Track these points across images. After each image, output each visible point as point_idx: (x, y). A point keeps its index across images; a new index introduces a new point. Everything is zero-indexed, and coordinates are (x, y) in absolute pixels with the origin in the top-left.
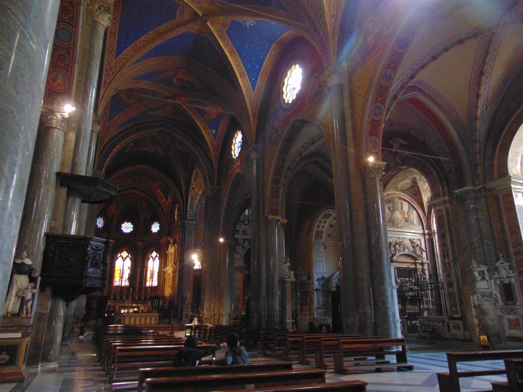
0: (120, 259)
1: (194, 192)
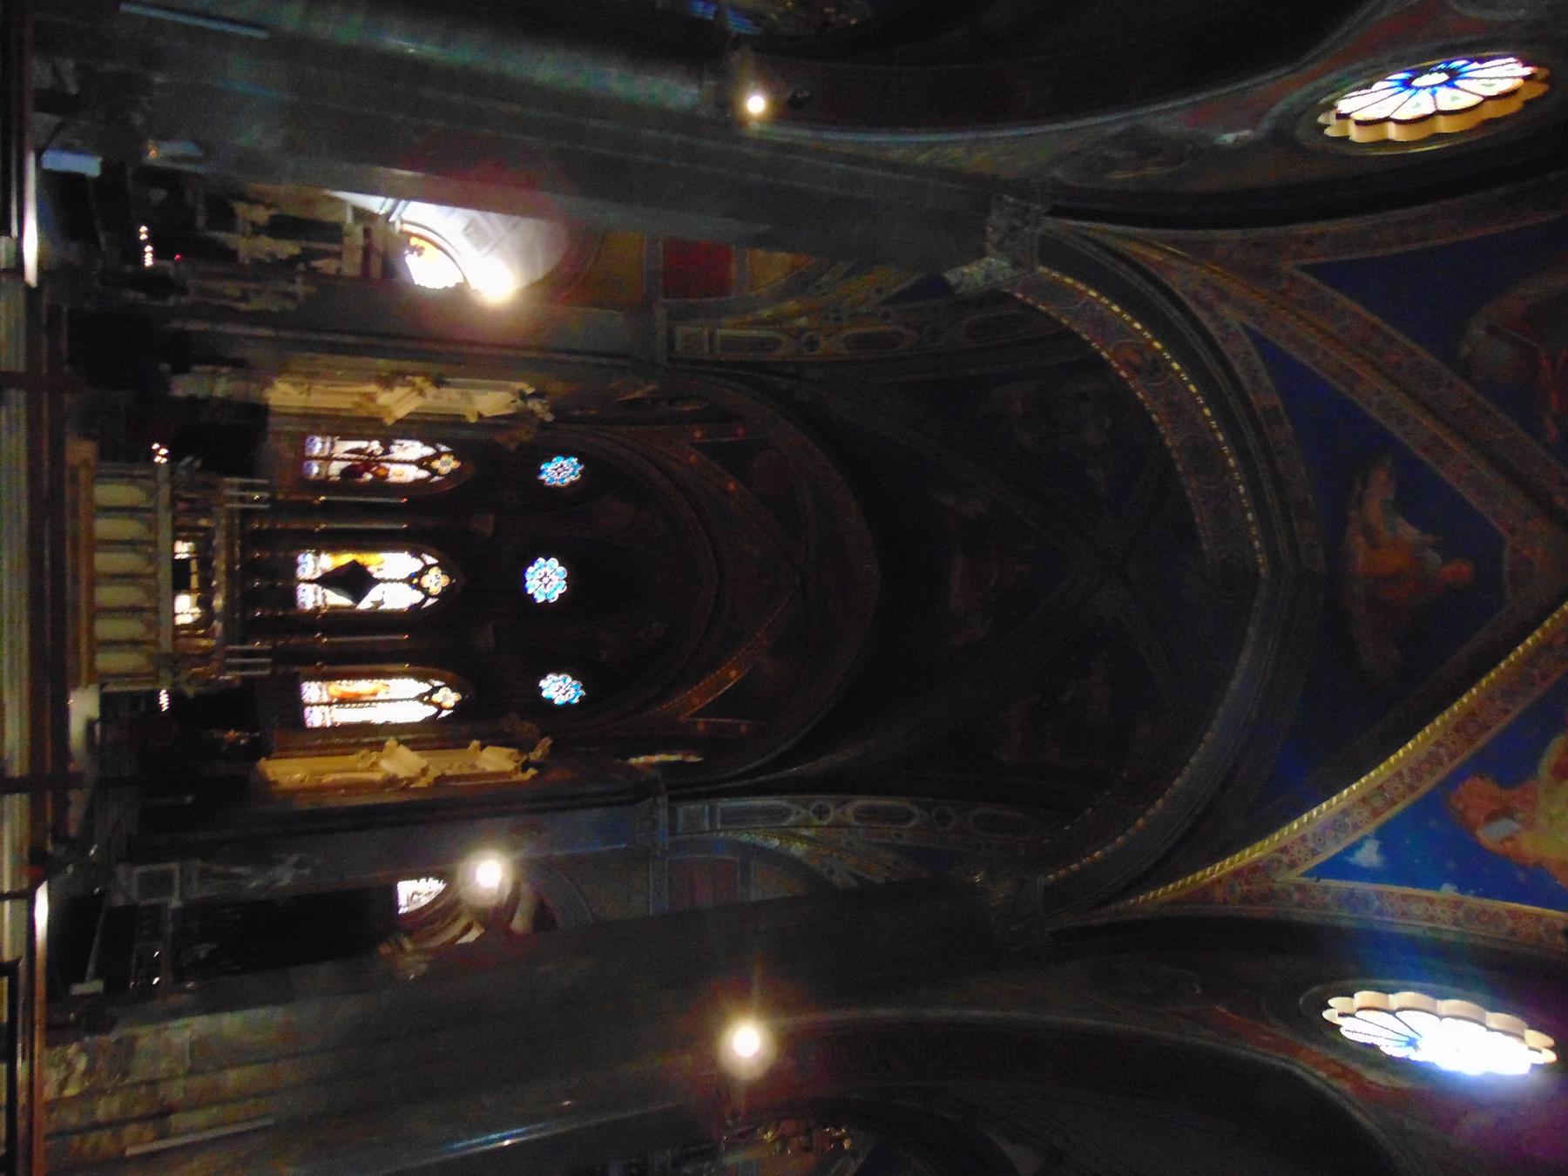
0: (416, 565)
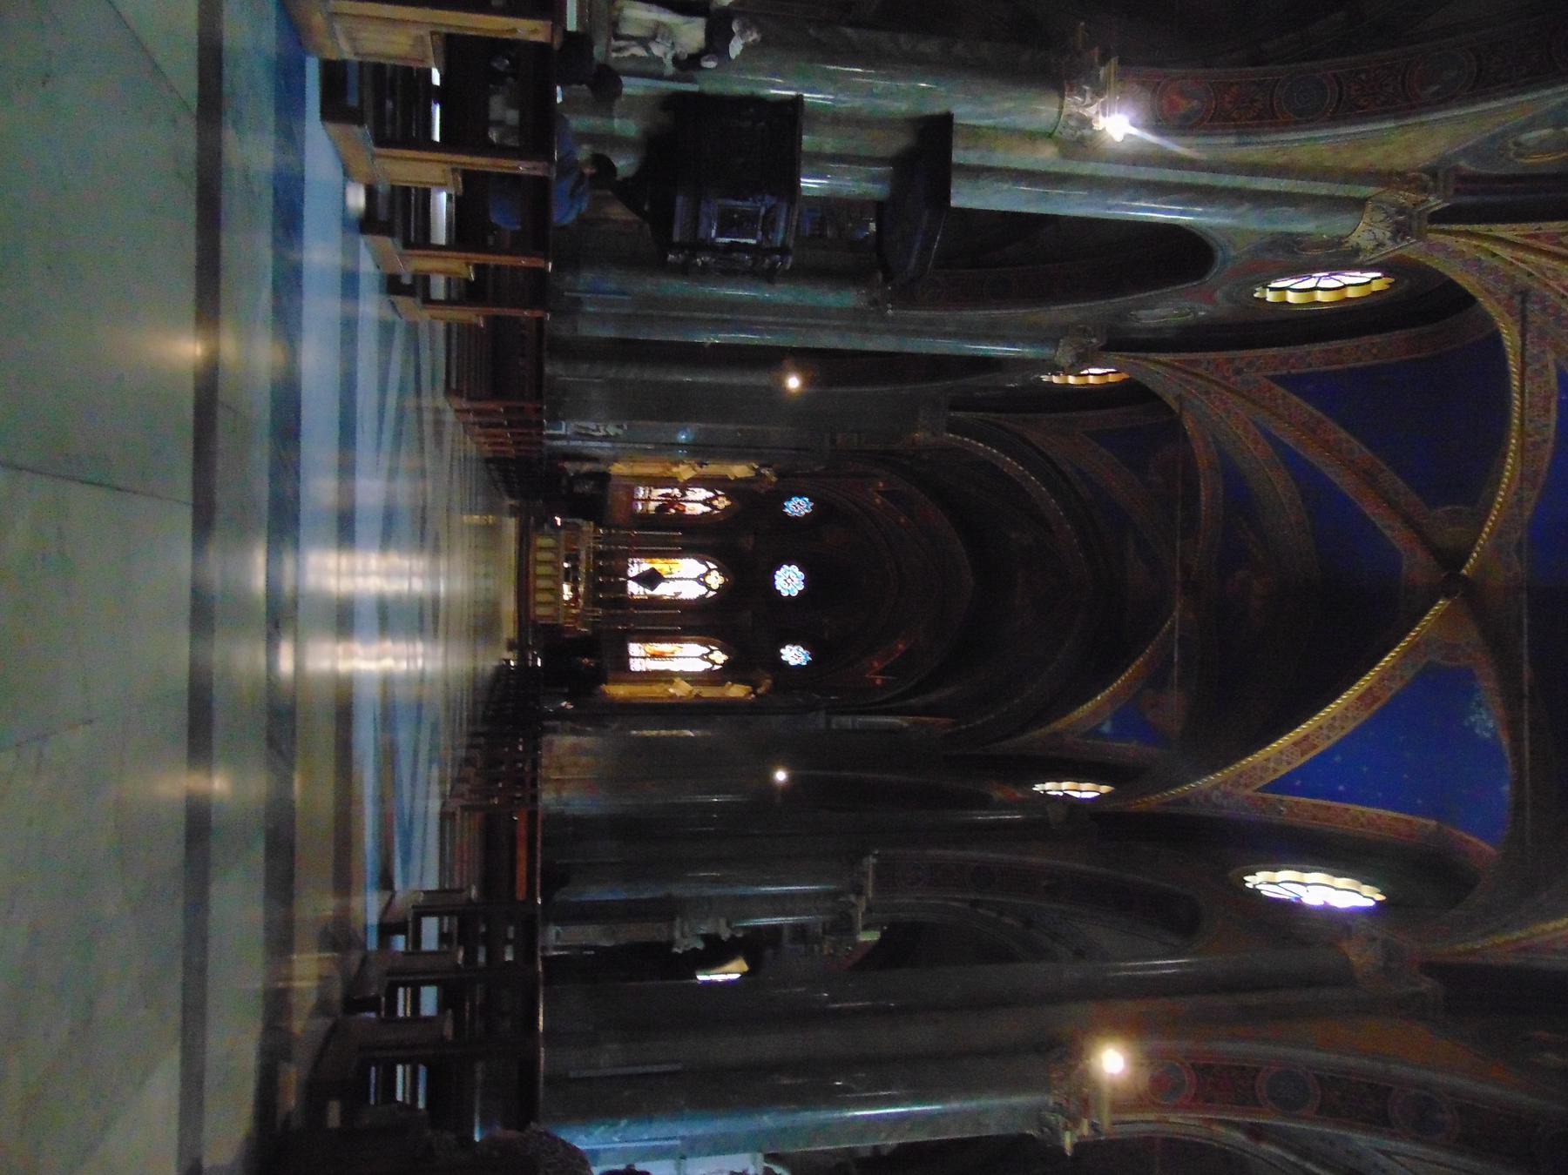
0: (703, 569)
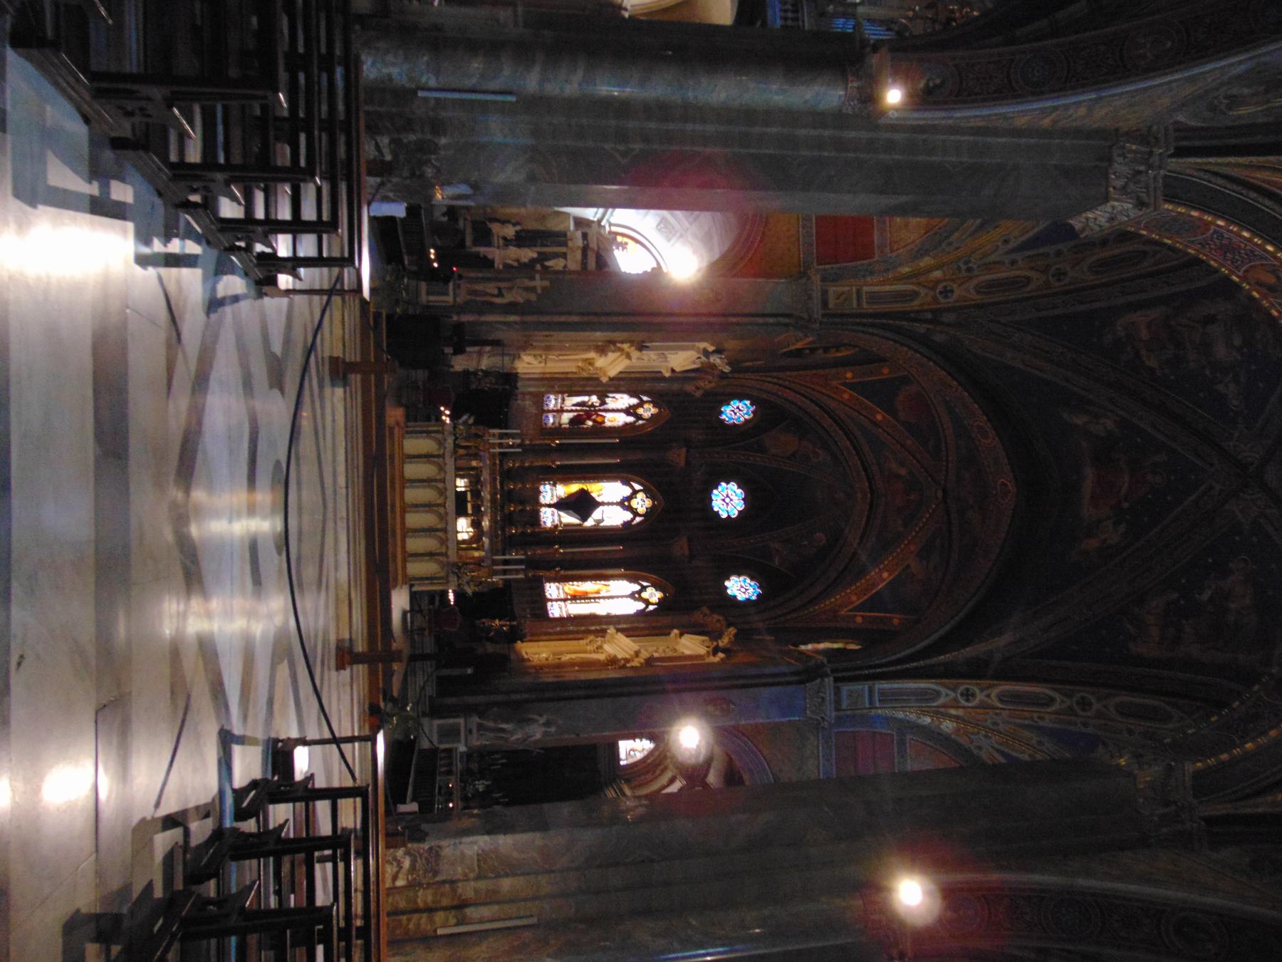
0: (627, 491)
1: (955, 700)
